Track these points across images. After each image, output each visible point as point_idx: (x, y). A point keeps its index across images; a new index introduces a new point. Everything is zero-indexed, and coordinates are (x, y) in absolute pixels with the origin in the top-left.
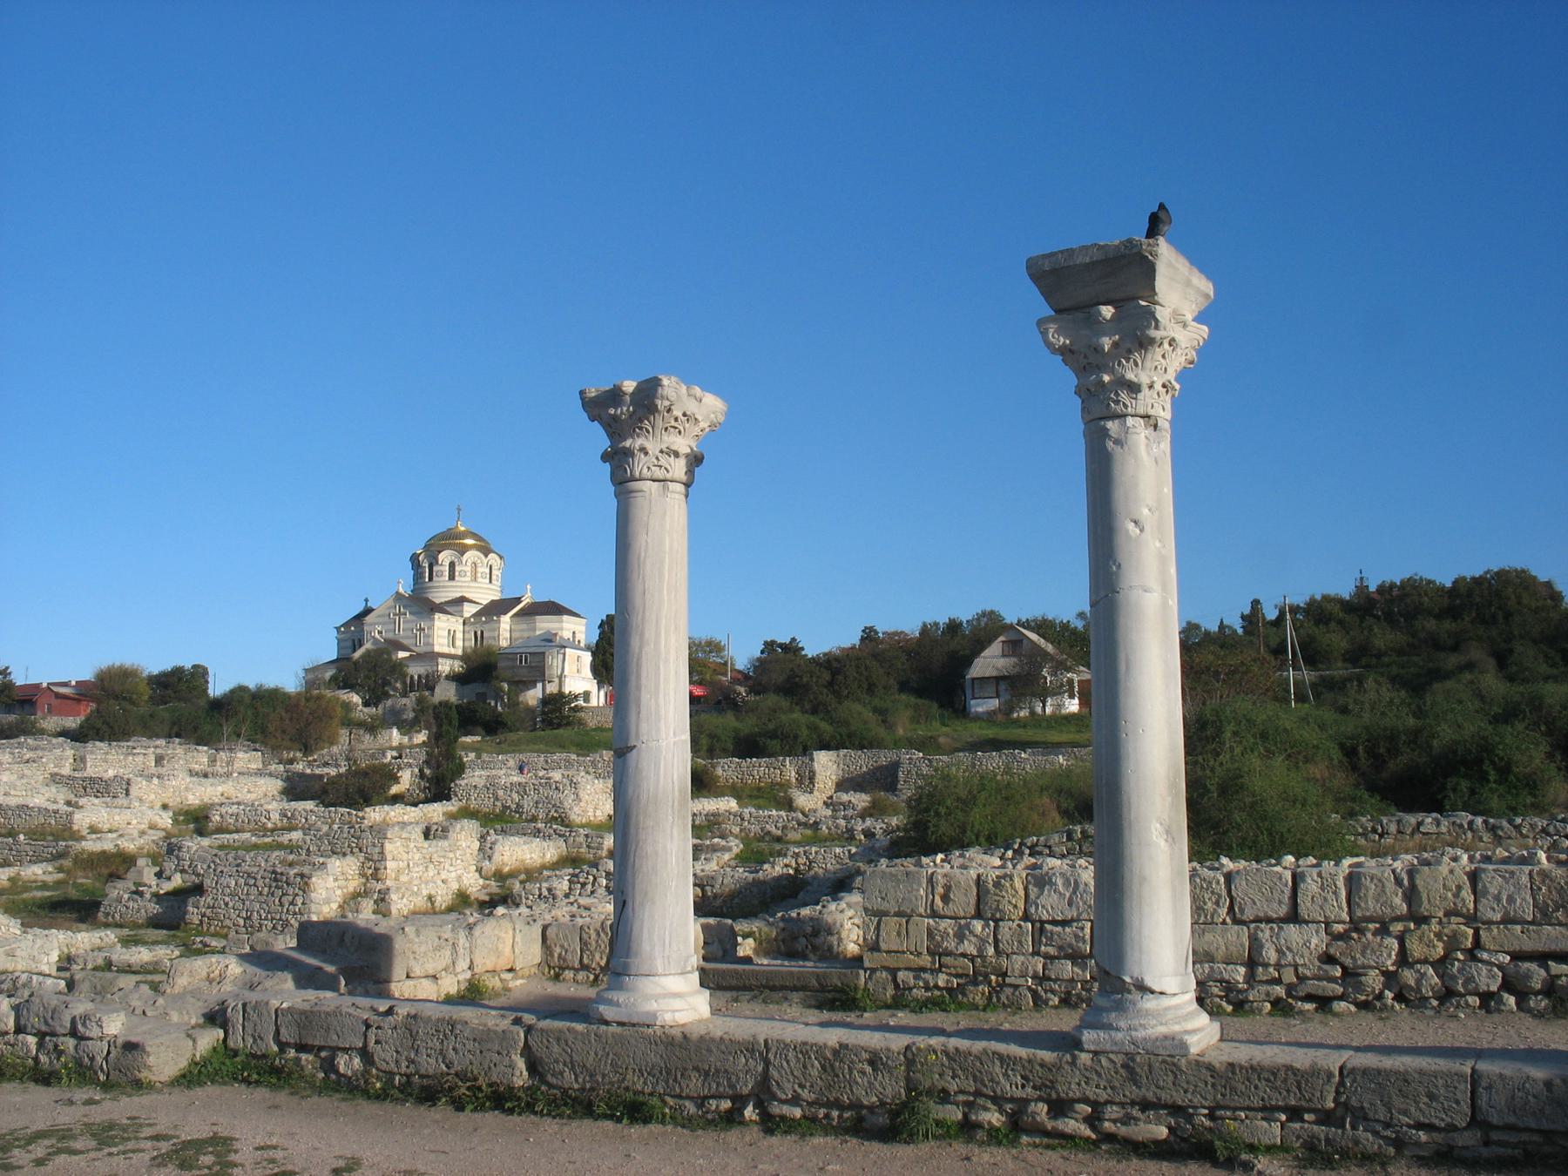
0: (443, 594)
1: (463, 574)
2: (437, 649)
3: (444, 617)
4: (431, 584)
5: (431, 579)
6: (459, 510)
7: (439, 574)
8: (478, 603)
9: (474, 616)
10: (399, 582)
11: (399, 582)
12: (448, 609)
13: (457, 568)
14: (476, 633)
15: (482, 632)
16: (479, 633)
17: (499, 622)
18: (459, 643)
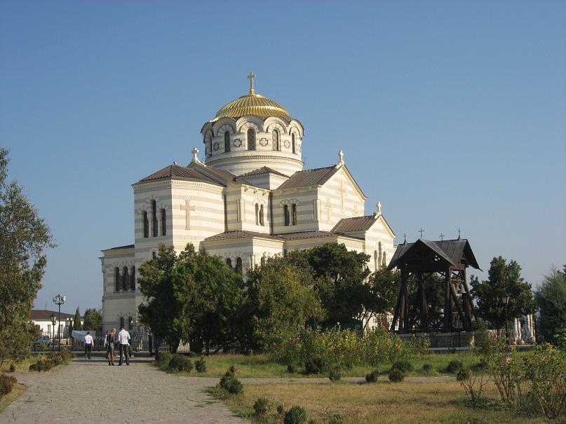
0: (244, 166)
1: (264, 142)
2: (246, 227)
3: (251, 190)
4: (228, 156)
5: (227, 149)
6: (250, 77)
7: (237, 143)
8: (283, 175)
9: (281, 187)
10: (194, 152)
11: (194, 152)
12: (250, 182)
13: (258, 136)
14: (286, 207)
15: (294, 206)
16: (290, 209)
17: (316, 193)
18: (266, 220)
